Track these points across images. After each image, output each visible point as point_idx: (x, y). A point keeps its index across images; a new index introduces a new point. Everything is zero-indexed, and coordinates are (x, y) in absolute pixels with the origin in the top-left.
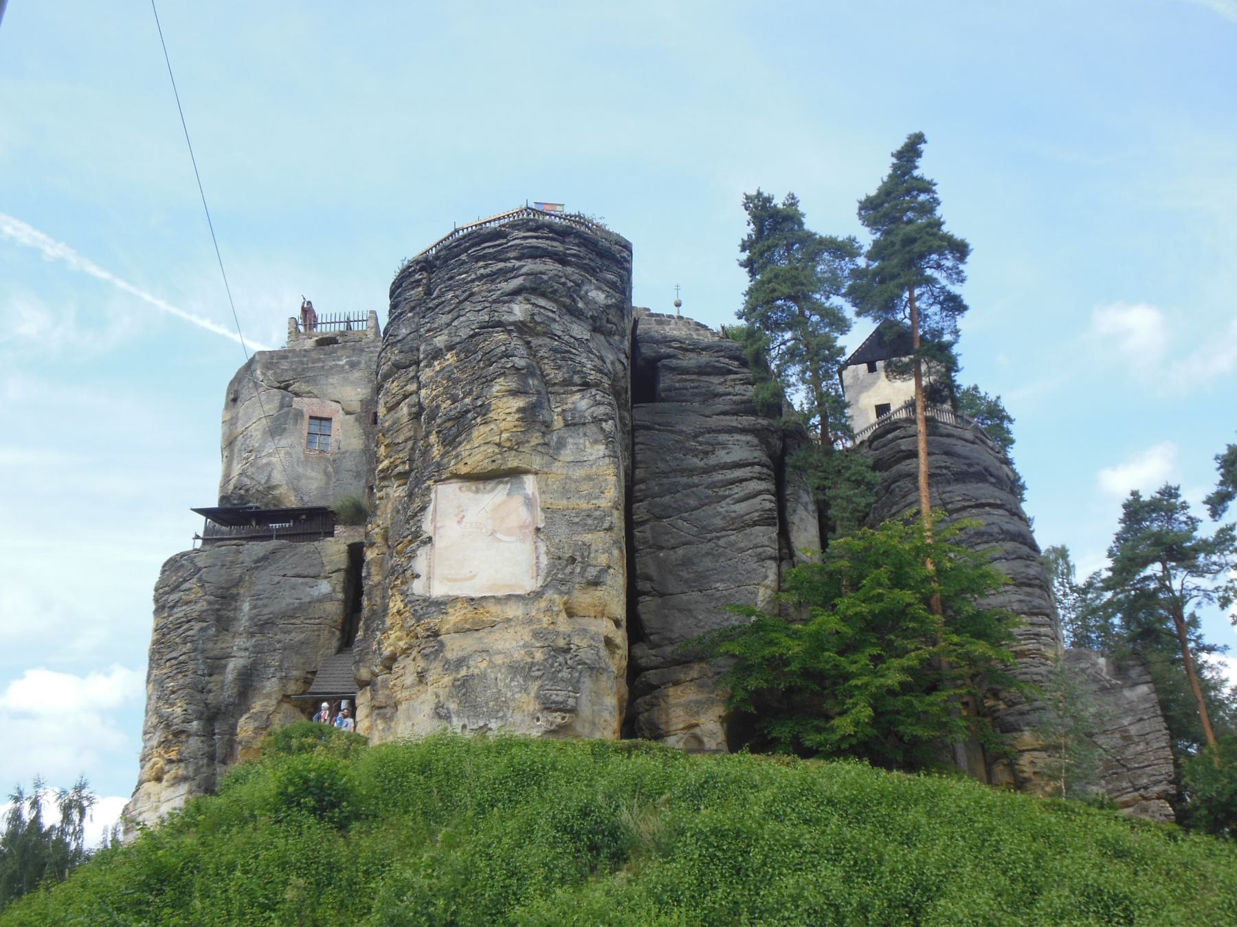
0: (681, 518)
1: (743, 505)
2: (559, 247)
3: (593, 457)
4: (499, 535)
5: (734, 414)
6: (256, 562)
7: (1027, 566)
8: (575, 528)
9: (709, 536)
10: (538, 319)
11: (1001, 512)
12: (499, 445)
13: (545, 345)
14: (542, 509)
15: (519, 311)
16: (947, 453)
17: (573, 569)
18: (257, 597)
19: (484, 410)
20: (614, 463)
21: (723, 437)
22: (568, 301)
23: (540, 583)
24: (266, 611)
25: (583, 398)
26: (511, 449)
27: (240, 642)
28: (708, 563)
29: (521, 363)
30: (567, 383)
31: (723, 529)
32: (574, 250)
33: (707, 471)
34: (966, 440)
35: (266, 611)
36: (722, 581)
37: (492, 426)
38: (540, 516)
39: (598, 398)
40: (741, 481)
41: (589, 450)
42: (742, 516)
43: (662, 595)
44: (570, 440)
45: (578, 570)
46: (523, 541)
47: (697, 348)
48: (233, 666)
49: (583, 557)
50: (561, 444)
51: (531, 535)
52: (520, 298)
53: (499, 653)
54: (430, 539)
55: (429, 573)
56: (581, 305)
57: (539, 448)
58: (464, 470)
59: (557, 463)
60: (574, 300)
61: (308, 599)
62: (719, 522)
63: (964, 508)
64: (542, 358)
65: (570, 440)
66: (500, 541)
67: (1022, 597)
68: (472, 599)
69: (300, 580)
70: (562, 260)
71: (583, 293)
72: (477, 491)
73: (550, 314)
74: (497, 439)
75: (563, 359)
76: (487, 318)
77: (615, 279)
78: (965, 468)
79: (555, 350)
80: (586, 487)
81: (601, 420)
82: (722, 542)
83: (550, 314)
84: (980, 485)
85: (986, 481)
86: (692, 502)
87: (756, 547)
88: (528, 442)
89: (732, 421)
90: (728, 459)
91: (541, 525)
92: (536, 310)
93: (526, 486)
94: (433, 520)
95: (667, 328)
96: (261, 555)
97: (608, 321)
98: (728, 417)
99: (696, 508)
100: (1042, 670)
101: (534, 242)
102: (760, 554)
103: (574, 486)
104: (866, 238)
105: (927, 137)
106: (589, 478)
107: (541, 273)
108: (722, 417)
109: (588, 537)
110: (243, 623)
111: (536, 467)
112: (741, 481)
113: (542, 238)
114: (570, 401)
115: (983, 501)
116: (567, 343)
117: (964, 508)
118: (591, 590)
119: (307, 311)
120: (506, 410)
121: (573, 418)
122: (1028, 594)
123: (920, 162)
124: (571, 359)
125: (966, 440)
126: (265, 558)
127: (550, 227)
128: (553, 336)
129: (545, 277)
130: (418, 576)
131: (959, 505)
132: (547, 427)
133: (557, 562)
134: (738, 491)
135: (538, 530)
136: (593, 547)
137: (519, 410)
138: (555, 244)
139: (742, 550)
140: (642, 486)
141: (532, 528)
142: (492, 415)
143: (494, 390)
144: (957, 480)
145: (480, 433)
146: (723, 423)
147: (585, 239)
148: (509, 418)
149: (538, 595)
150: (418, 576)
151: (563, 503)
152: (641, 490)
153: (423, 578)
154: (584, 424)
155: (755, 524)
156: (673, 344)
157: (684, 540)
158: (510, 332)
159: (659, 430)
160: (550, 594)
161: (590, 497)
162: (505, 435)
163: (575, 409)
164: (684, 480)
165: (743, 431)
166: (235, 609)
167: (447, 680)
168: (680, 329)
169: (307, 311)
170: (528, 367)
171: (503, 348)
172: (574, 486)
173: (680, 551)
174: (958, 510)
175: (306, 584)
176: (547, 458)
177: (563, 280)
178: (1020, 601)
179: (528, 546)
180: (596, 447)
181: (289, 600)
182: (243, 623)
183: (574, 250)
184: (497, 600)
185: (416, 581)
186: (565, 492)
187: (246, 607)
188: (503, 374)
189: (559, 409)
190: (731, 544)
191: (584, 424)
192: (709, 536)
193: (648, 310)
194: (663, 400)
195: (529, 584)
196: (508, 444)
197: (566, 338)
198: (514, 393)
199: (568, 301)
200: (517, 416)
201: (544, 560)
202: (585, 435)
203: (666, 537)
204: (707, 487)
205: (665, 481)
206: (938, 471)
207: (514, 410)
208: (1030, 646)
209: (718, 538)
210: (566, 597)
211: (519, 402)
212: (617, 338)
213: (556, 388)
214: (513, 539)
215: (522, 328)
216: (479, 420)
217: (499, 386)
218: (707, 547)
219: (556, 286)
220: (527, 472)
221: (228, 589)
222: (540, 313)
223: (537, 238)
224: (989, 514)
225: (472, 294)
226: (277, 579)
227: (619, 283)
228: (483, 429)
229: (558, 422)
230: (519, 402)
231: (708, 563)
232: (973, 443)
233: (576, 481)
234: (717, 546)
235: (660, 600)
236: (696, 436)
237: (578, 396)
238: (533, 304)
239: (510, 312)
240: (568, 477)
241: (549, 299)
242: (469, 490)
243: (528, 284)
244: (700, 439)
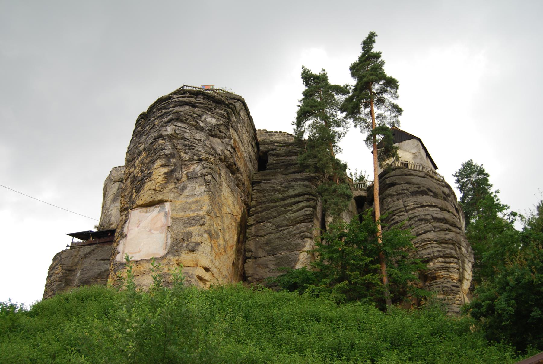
0: (269, 222)
1: (296, 214)
2: (193, 100)
3: (199, 192)
4: (153, 231)
5: (299, 173)
6: (85, 255)
7: (446, 234)
8: (186, 225)
9: (280, 229)
10: (177, 132)
11: (435, 209)
12: (155, 190)
13: (181, 143)
14: (172, 218)
15: (170, 130)
16: (408, 183)
17: (182, 245)
18: (83, 270)
20: (208, 194)
21: (293, 183)
22: (194, 123)
23: (166, 252)
24: (86, 276)
25: (198, 166)
26: (160, 191)
29: (167, 152)
30: (191, 159)
31: (287, 225)
32: (201, 101)
33: (283, 199)
34: (420, 177)
35: (86, 276)
37: (153, 182)
38: (170, 220)
39: (205, 165)
40: (298, 202)
41: (197, 189)
42: (296, 219)
43: (255, 258)
44: (189, 185)
45: (185, 244)
46: (162, 233)
47: (287, 144)
49: (188, 238)
50: (184, 188)
51: (165, 230)
52: (170, 124)
53: (145, 285)
54: (126, 235)
55: (123, 251)
56: (202, 124)
57: (173, 190)
58: (141, 203)
59: (182, 196)
60: (197, 123)
61: (103, 270)
62: (286, 222)
63: (415, 208)
64: (179, 149)
65: (189, 185)
66: (153, 233)
67: (440, 249)
68: (137, 261)
69: (103, 262)
70: (194, 106)
71: (203, 119)
72: (146, 212)
73: (184, 129)
74: (154, 187)
75: (189, 149)
76: (157, 134)
77: (223, 112)
78: (416, 189)
79: (185, 146)
80: (194, 206)
81: (205, 175)
82: (285, 232)
84: (425, 196)
85: (428, 195)
86: (275, 214)
87: (301, 232)
88: (167, 187)
89: (298, 176)
90: (293, 193)
91: (170, 225)
92: (177, 128)
93: (166, 208)
95: (274, 137)
96: (88, 251)
97: (220, 132)
98: (296, 174)
99: (276, 217)
100: (449, 285)
101: (181, 99)
102: (302, 236)
103: (188, 206)
104: (352, 82)
105: (377, 33)
106: (196, 202)
108: (294, 174)
109: (191, 229)
111: (171, 199)
112: (298, 202)
113: (185, 97)
114: (192, 168)
115: (425, 204)
116: (192, 142)
117: (415, 208)
118: (191, 254)
120: (159, 172)
121: (192, 175)
122: (444, 247)
123: (374, 45)
124: (193, 149)
125: (420, 177)
126: (89, 253)
127: (190, 92)
128: (185, 139)
129: (182, 113)
130: (119, 253)
131: (412, 207)
132: (178, 180)
133: (175, 241)
134: (295, 207)
135: (169, 227)
136: (194, 234)
137: (165, 173)
138: (191, 99)
139: (294, 235)
140: (253, 209)
141: (166, 227)
142: (153, 177)
143: (155, 165)
144: (412, 195)
145: (148, 185)
146: (294, 177)
147: (207, 96)
148: (160, 177)
149: (164, 257)
151: (182, 214)
152: (253, 211)
153: (121, 253)
154: (197, 178)
155: (302, 222)
156: (276, 144)
157: (268, 232)
158: (165, 139)
159: (264, 183)
160: (170, 257)
161: (196, 210)
162: (158, 185)
164: (272, 204)
165: (303, 180)
166: (74, 276)
168: (280, 137)
170: (170, 154)
171: (161, 146)
172: (188, 206)
173: (266, 237)
174: (412, 209)
175: (105, 263)
176: (176, 194)
177: (191, 114)
178: (438, 251)
179: (163, 235)
180: (201, 187)
181: (96, 270)
183: (201, 101)
184: (147, 261)
185: (118, 255)
186: (184, 209)
187: (78, 274)
189: (186, 172)
191: (197, 178)
192: (280, 229)
193: (266, 130)
194: (268, 169)
195: (162, 253)
196: (158, 189)
197: (192, 140)
198: (163, 166)
199: (194, 123)
200: (163, 176)
201: (170, 241)
203: (261, 231)
204: (282, 207)
205: (264, 205)
206: (403, 192)
208: (443, 273)
209: (284, 230)
210: (177, 258)
211: (165, 170)
212: (227, 140)
213: (186, 162)
214: (158, 232)
215: (171, 137)
217: (158, 163)
218: (277, 235)
219: (187, 117)
220: (166, 201)
221: (72, 267)
222: (178, 129)
223: (183, 97)
224: (428, 210)
225: (154, 125)
226: (93, 262)
227: (226, 114)
228: (149, 183)
229: (184, 178)
230: (165, 170)
231: (278, 242)
232: (424, 177)
233: (190, 204)
234: (284, 234)
235: (254, 260)
236: (281, 184)
237: (196, 165)
238: (176, 126)
240: (187, 202)
241: (185, 123)
242: (144, 212)
243: (174, 117)
244: (283, 185)
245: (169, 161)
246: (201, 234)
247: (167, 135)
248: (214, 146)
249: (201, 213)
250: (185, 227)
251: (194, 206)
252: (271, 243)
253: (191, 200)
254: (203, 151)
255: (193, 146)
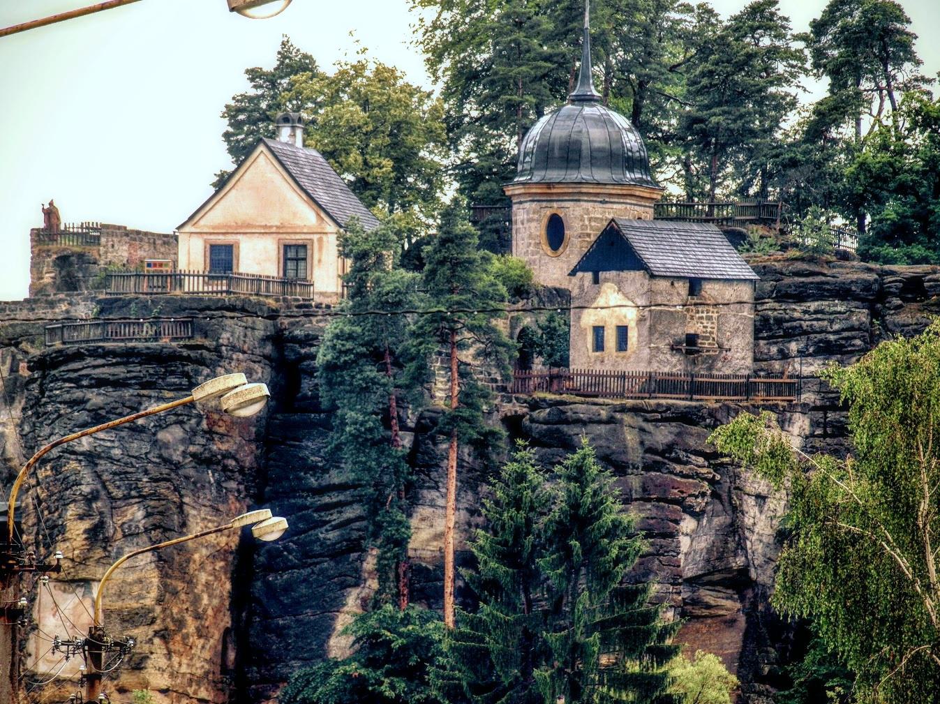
12: (72, 560)
19: (62, 529)
20: (158, 567)
25: (139, 510)
26: (80, 563)
28: (303, 590)
30: (126, 497)
31: (321, 555)
36: (310, 607)
38: (101, 616)
62: (317, 548)
72: (64, 591)
74: (70, 555)
75: (121, 480)
79: (115, 474)
80: (136, 589)
82: (316, 569)
83: (109, 444)
90: (336, 481)
94: (39, 611)
95: (314, 319)
106: (140, 581)
107: (101, 408)
114: (130, 512)
119: (51, 213)
120: (77, 530)
130: (30, 655)
134: (335, 517)
136: (139, 640)
137: (86, 531)
139: (330, 578)
142: (68, 535)
150: (30, 655)
151: (118, 605)
153: (33, 657)
162: (77, 552)
163: (131, 520)
169: (51, 213)
188: (74, 501)
190: (322, 571)
192: (309, 561)
196: (78, 560)
198: (81, 518)
200: (84, 536)
202: (137, 544)
207: (81, 531)
209: (315, 564)
210: (115, 682)
213: (119, 503)
216: (60, 537)
217: (72, 511)
220: (94, 580)
222: (100, 445)
230: (86, 525)
231: (303, 590)
233: (130, 584)
237: (136, 507)
240: (124, 581)
245: (90, 507)
246: (151, 640)
247: (82, 454)
248: (165, 455)
249: (149, 602)
250: (126, 628)
251: (136, 589)
252: (293, 591)
253: (131, 577)
254: (145, 480)
255: (126, 473)
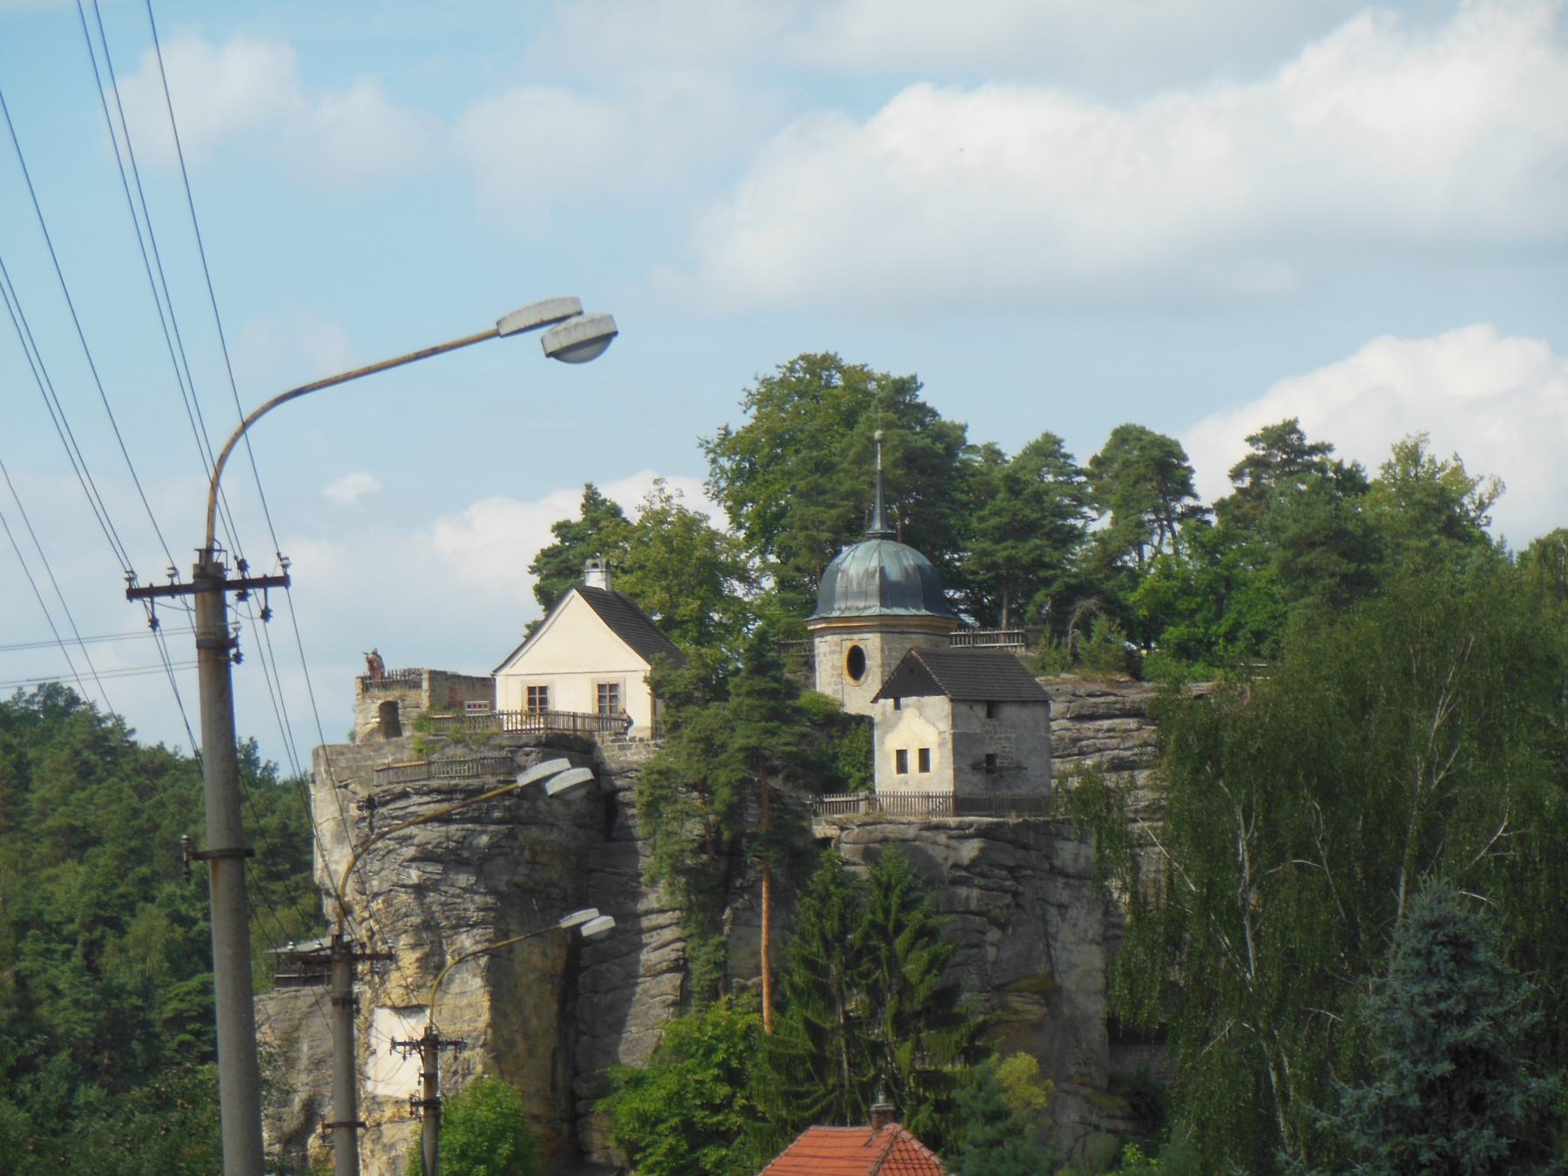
1: (658, 953)
15: (414, 875)
24: (319, 1051)
27: (303, 1078)
35: (319, 1051)
40: (661, 927)
48: (298, 1100)
79: (443, 904)
80: (468, 1014)
110: (304, 1062)
137: (418, 960)
145: (395, 976)
167: (385, 1158)
182: (304, 1062)
187: (305, 1048)
215: (419, 890)
230: (418, 954)
239: (409, 876)
251: (468, 1014)
